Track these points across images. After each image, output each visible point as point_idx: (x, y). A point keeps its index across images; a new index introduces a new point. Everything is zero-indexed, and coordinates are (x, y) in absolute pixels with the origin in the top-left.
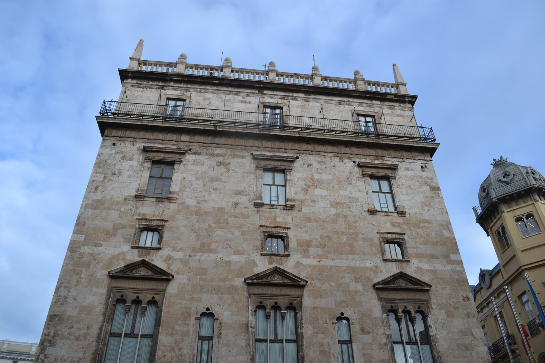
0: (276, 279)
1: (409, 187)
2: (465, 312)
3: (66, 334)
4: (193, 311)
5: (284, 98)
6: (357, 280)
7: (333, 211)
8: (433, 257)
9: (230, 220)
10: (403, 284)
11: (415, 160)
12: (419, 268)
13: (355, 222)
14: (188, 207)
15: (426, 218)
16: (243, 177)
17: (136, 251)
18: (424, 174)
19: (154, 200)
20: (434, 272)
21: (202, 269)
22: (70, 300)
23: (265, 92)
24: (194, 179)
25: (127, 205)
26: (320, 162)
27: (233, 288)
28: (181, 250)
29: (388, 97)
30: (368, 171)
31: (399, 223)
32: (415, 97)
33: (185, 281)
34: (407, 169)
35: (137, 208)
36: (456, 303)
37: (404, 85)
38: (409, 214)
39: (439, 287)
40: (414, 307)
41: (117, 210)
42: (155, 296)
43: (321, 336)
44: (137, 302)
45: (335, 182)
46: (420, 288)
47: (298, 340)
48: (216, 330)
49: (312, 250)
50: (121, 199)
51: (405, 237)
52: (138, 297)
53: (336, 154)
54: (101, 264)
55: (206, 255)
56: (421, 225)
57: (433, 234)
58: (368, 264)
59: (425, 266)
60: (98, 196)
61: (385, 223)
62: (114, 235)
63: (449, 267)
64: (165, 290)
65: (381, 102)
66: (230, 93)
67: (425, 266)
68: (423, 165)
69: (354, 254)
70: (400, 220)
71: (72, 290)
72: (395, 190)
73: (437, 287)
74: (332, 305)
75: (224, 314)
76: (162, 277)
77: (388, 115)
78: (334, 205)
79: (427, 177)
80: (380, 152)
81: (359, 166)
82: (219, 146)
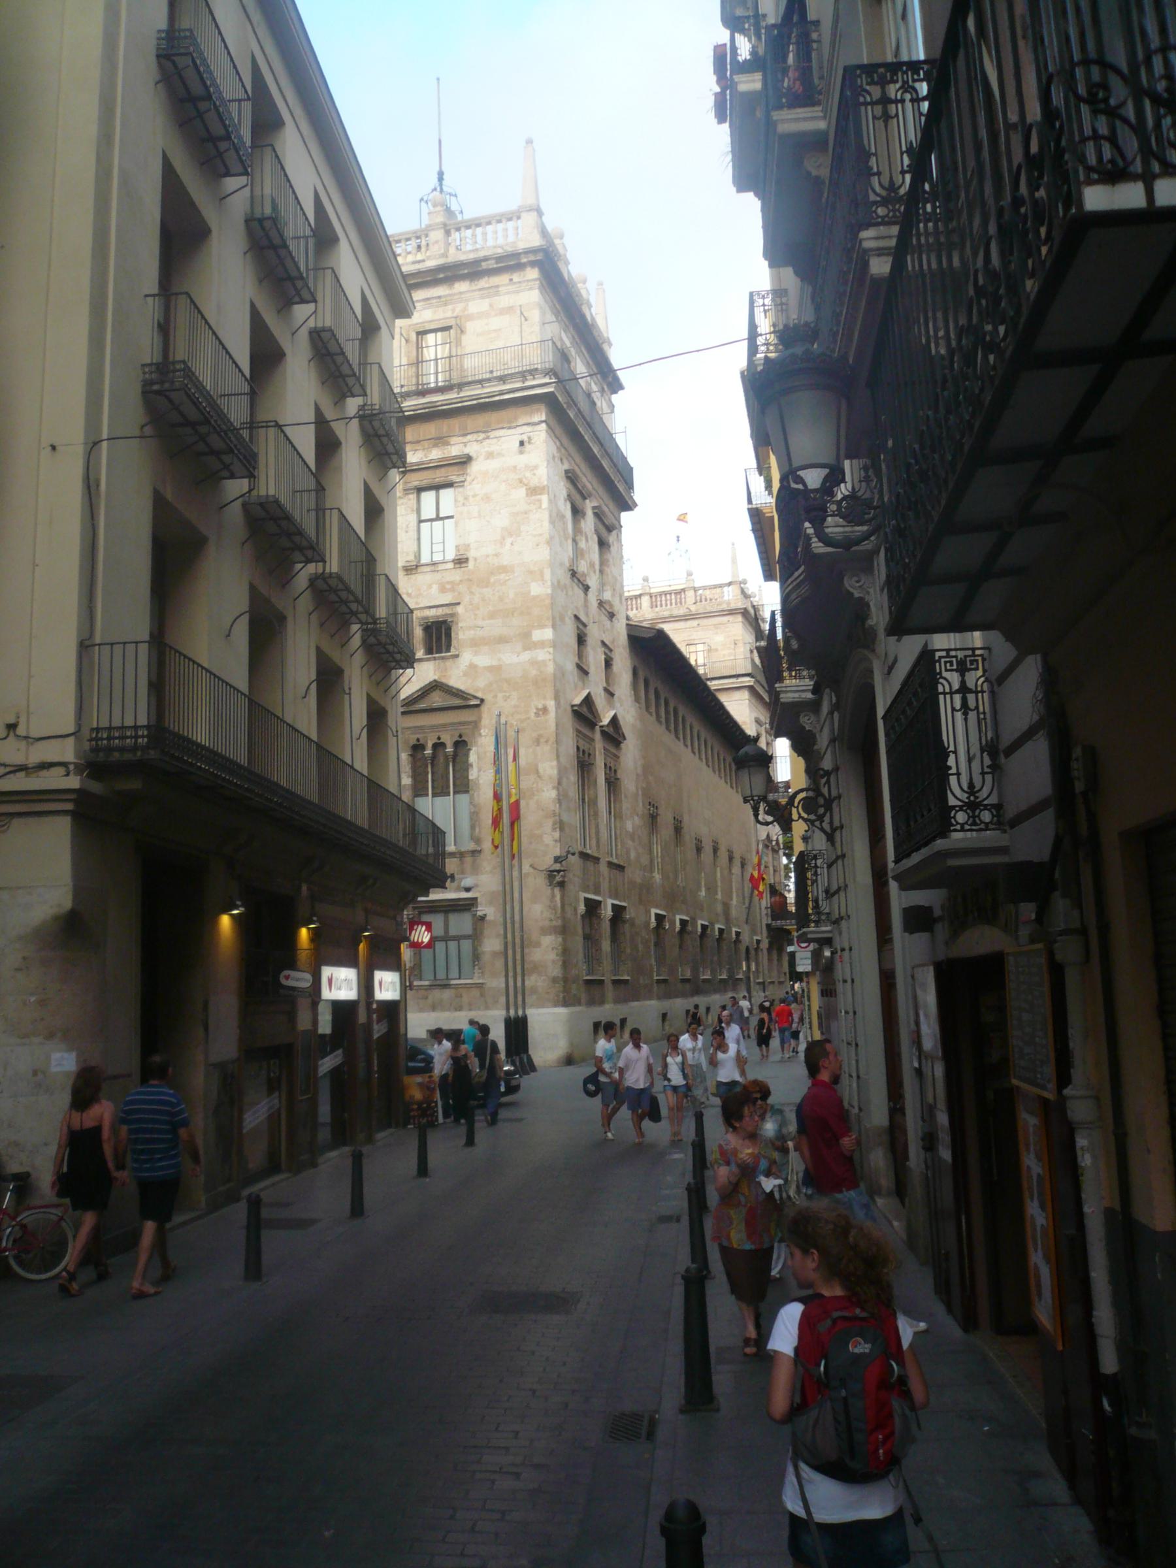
1: (487, 498)
2: (535, 735)
8: (502, 640)
10: (437, 699)
11: (509, 428)
12: (472, 667)
15: (505, 561)
18: (523, 460)
29: (484, 265)
31: (452, 583)
34: (490, 455)
36: (522, 721)
38: (475, 559)
39: (500, 695)
40: (452, 736)
46: (464, 703)
51: (460, 610)
56: (492, 580)
57: (511, 595)
59: (483, 660)
61: (430, 587)
63: (526, 656)
65: (471, 281)
67: (483, 660)
68: (525, 437)
70: (456, 575)
73: (495, 696)
77: (481, 315)
79: (527, 466)
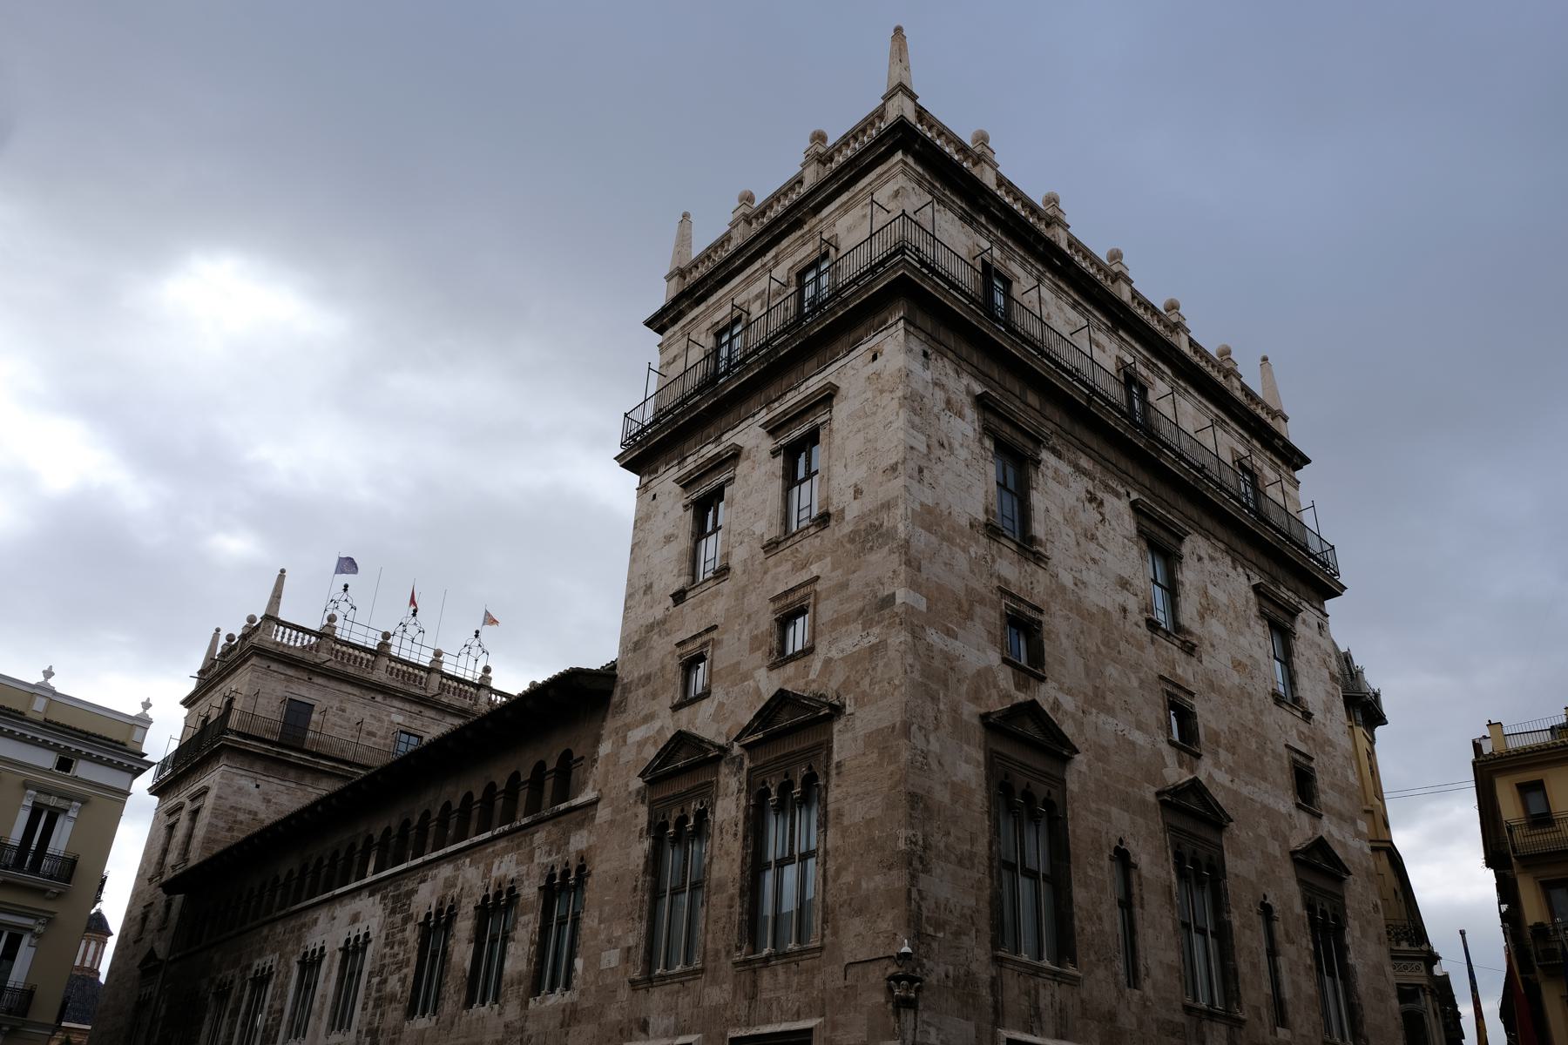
0: (1193, 804)
3: (942, 845)
4: (1104, 841)
5: (1148, 364)
6: (1275, 833)
7: (1236, 678)
9: (1123, 645)
13: (1261, 712)
14: (1063, 588)
16: (1124, 546)
17: (1009, 670)
19: (1013, 547)
20: (1344, 845)
21: (1104, 748)
22: (935, 766)
23: (1121, 333)
24: (1061, 520)
25: (977, 542)
26: (1212, 559)
27: (1143, 802)
28: (1069, 692)
30: (1269, 608)
32: (1307, 461)
33: (1084, 768)
35: (994, 561)
37: (1285, 419)
41: (965, 550)
42: (1053, 791)
43: (1248, 932)
44: (1028, 796)
45: (1231, 613)
47: (1223, 933)
48: (1135, 890)
49: (1223, 755)
50: (964, 522)
51: (1313, 765)
52: (1028, 785)
53: (1230, 550)
54: (965, 687)
55: (1102, 717)
58: (1283, 810)
60: (928, 497)
62: (970, 616)
64: (1064, 781)
66: (1075, 306)
69: (1265, 779)
71: (932, 739)
72: (1299, 663)
74: (1253, 878)
75: (1143, 858)
76: (1058, 748)
78: (1238, 665)
80: (1276, 571)
81: (1256, 589)
82: (1085, 449)
